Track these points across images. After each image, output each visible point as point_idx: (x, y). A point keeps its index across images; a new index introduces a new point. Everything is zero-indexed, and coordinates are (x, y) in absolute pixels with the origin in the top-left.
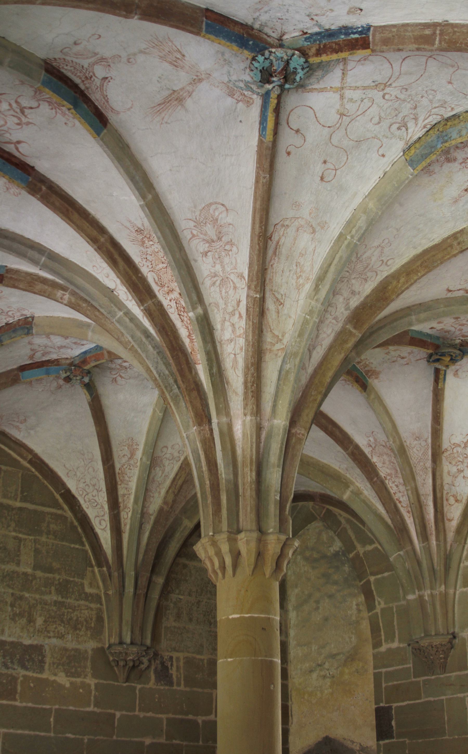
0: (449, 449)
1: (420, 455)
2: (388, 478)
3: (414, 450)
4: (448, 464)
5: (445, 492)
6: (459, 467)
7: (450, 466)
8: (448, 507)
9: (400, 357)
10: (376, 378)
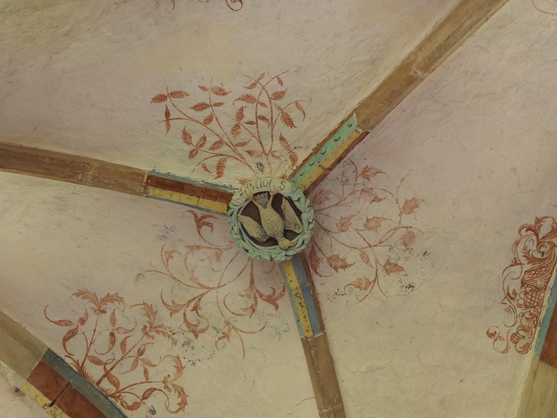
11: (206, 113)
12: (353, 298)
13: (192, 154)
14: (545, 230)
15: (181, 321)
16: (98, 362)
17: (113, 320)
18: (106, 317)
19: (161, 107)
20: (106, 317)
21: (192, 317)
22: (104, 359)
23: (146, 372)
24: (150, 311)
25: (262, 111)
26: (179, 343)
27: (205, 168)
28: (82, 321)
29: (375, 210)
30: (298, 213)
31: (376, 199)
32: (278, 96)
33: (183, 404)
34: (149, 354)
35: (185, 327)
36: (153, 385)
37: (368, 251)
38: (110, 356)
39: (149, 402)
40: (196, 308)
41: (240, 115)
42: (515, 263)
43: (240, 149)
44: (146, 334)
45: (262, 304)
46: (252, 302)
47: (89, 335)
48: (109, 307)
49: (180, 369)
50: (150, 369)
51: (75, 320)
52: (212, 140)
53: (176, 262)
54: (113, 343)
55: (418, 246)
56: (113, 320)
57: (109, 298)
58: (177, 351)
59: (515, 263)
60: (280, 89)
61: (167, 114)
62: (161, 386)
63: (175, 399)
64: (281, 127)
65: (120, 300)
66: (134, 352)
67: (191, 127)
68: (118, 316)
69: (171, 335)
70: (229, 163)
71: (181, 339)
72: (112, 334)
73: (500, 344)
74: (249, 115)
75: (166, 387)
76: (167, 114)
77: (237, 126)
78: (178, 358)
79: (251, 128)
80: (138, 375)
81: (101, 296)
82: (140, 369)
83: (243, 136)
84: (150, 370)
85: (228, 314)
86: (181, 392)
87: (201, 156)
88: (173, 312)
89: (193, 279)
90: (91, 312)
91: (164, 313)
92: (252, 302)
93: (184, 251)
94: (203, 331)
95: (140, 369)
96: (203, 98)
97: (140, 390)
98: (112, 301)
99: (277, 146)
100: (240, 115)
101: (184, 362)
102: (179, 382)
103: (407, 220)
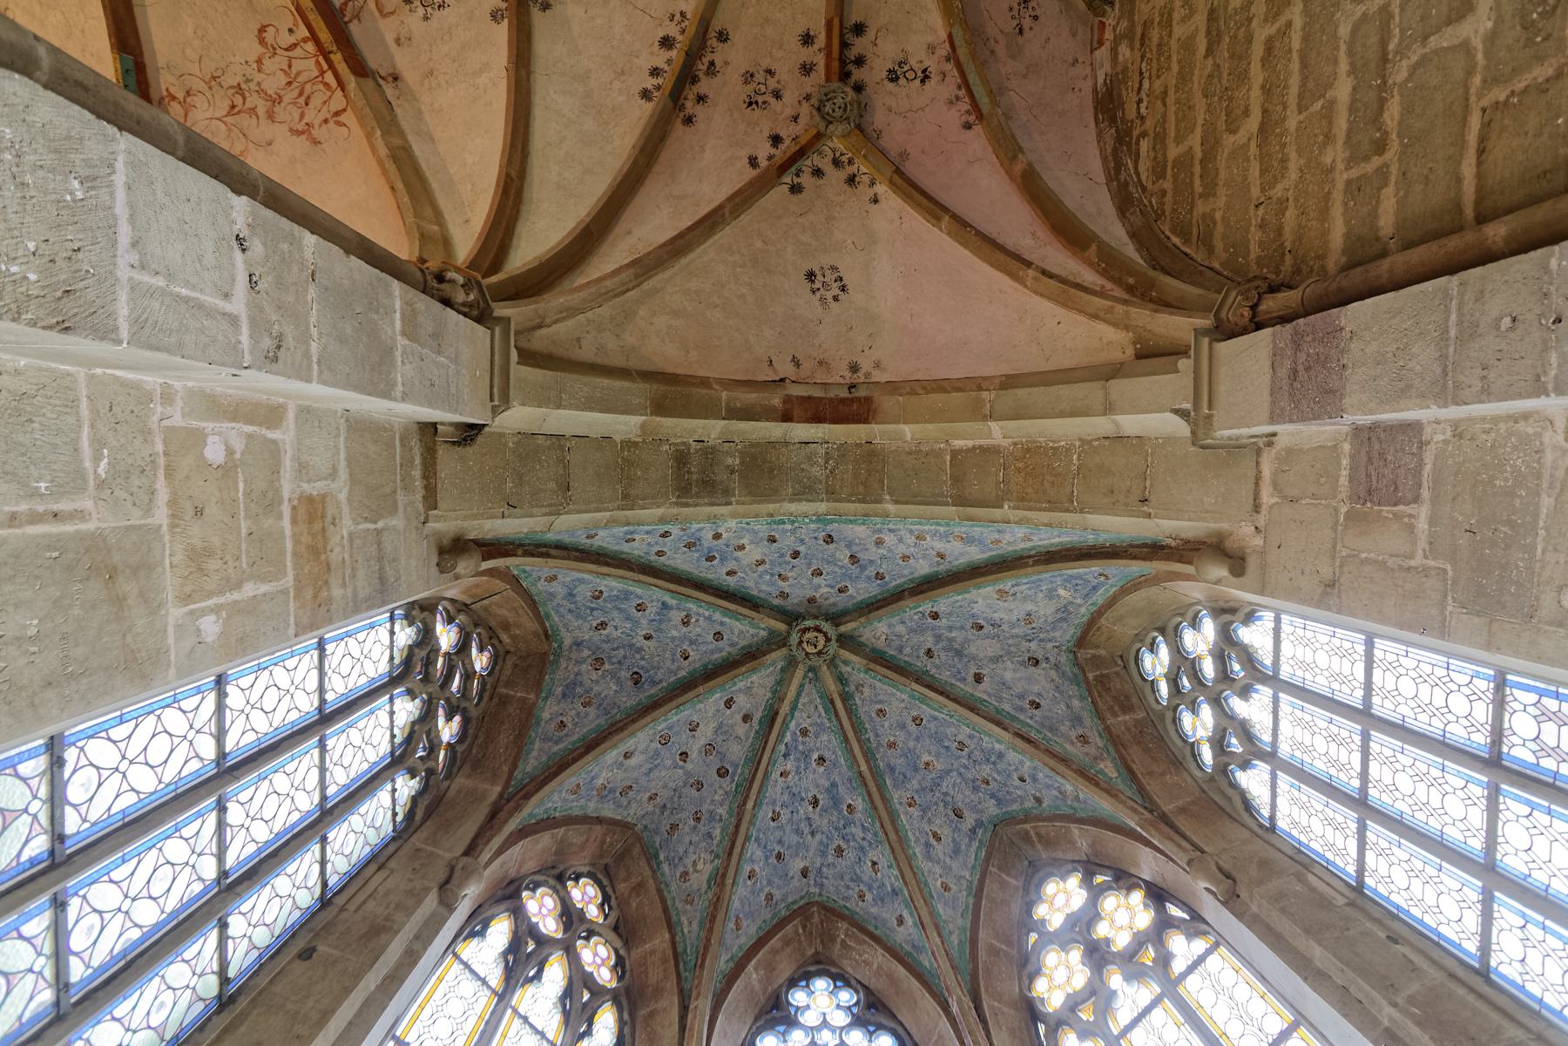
15: (248, 100)
16: (326, 85)
17: (302, 116)
18: (306, 120)
20: (306, 120)
21: (238, 100)
22: (321, 87)
23: (290, 67)
24: (271, 116)
26: (255, 82)
28: (326, 121)
33: (262, 29)
34: (284, 80)
35: (247, 94)
36: (286, 53)
38: (315, 87)
39: (292, 40)
44: (280, 97)
45: (180, 95)
46: (188, 100)
47: (325, 109)
48: (301, 127)
49: (259, 61)
50: (286, 68)
51: (331, 124)
54: (309, 97)
56: (302, 116)
57: (299, 133)
62: (279, 51)
63: (269, 35)
65: (291, 130)
66: (295, 85)
68: (297, 117)
69: (261, 91)
71: (253, 85)
72: (307, 104)
75: (274, 49)
78: (259, 71)
80: (297, 65)
81: (304, 137)
82: (294, 70)
86: (262, 41)
89: (230, 130)
90: (316, 127)
91: (261, 111)
92: (188, 100)
97: (298, 52)
101: (255, 66)
102: (260, 50)
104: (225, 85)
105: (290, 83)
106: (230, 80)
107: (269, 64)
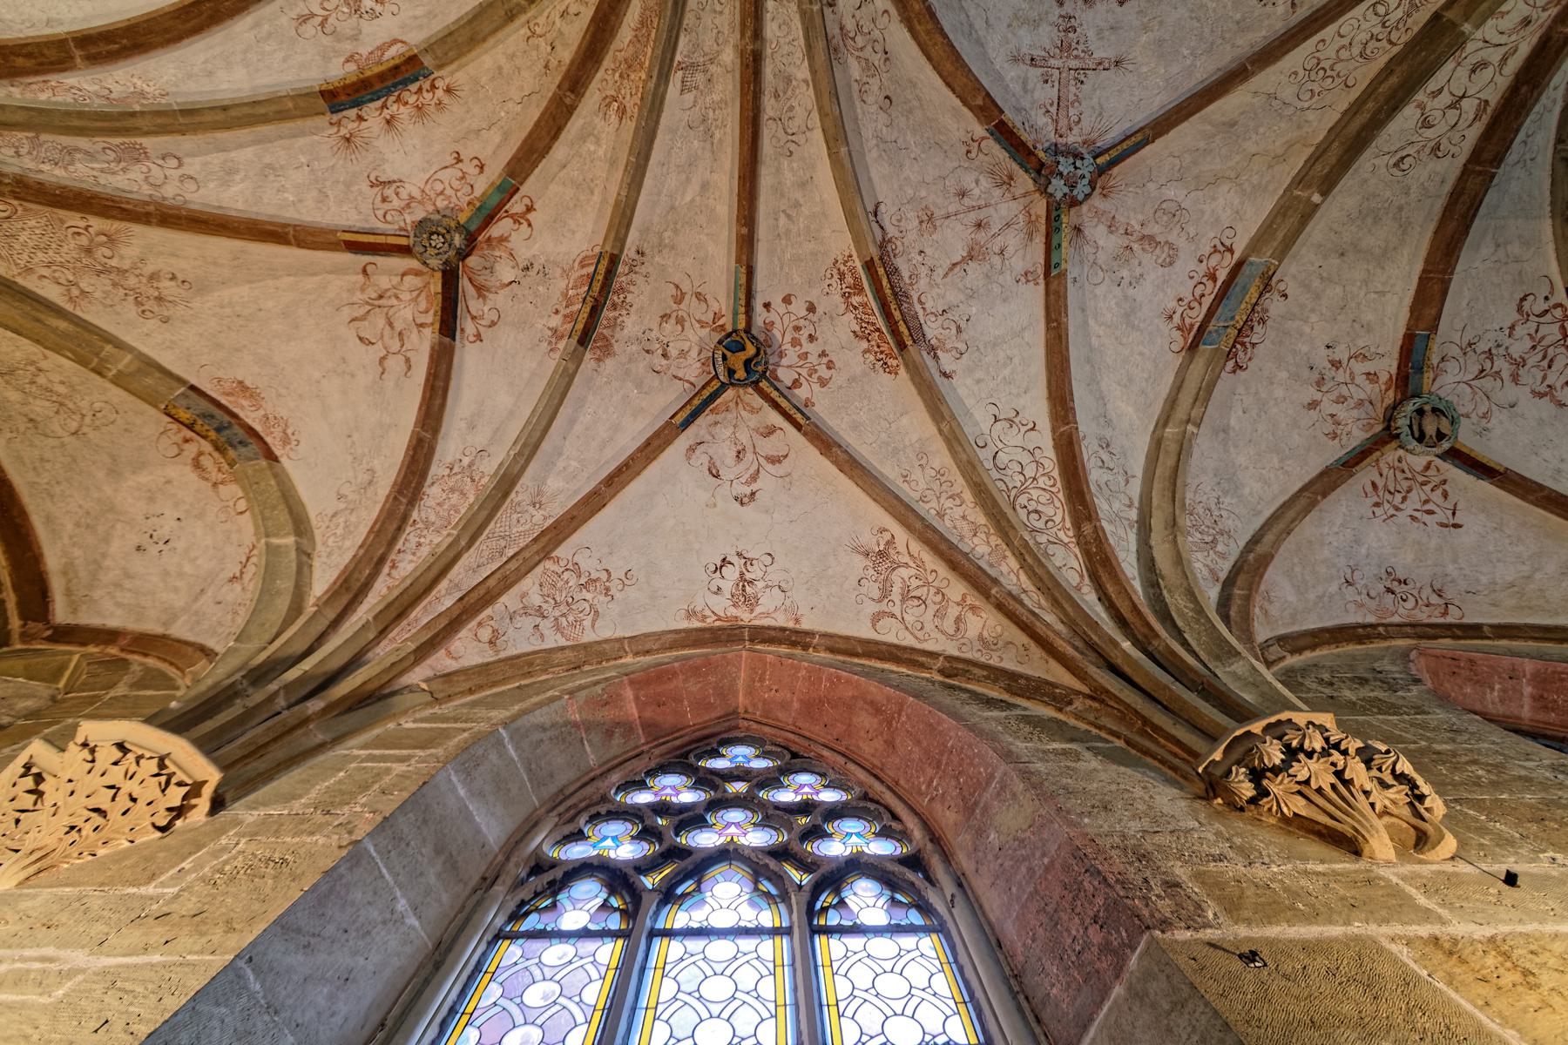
0: (562, 563)
1: (514, 530)
2: (420, 525)
3: (515, 516)
4: (537, 582)
5: (488, 611)
6: (545, 606)
7: (537, 587)
8: (471, 635)
9: (664, 350)
10: (599, 360)
11: (1427, 507)
12: (1373, 350)
13: (1445, 482)
14: (1231, 364)
15: (1496, 363)
17: (1544, 378)
18: (1548, 382)
19: (1457, 520)
20: (1548, 382)
21: (1488, 365)
23: (1537, 331)
24: (1515, 378)
25: (1388, 496)
27: (1438, 470)
29: (1335, 409)
30: (1410, 427)
31: (1333, 416)
32: (1377, 505)
33: (1523, 299)
34: (1529, 344)
36: (1537, 319)
37: (1348, 381)
38: (1558, 351)
40: (1483, 371)
41: (1404, 499)
42: (1254, 345)
43: (1410, 476)
48: (1543, 389)
49: (1512, 328)
52: (1427, 488)
53: (1483, 409)
55: (1315, 376)
56: (1544, 378)
57: (1541, 395)
58: (1507, 342)
59: (1254, 345)
60: (1376, 509)
61: (1454, 514)
64: (1380, 483)
65: (1533, 392)
66: (1539, 348)
67: (1440, 500)
69: (1508, 356)
70: (1419, 469)
71: (1502, 351)
72: (1550, 367)
73: (1282, 286)
74: (1398, 497)
76: (1454, 514)
77: (1408, 492)
79: (1398, 488)
80: (1544, 330)
81: (1547, 399)
82: (1540, 335)
83: (1405, 484)
84: (1532, 332)
85: (1461, 360)
86: (1520, 309)
87: (1437, 480)
88: (1498, 373)
89: (1475, 393)
90: (1559, 388)
91: (1505, 374)
93: (1473, 415)
94: (1484, 352)
95: (1540, 335)
96: (1426, 518)
97: (1548, 317)
98: (1539, 393)
99: (1385, 472)
100: (1404, 499)
101: (1507, 332)
102: (1517, 316)
103: (1318, 396)
104: (1479, 351)
105: (1534, 347)
106: (1482, 346)
107: (1520, 331)
